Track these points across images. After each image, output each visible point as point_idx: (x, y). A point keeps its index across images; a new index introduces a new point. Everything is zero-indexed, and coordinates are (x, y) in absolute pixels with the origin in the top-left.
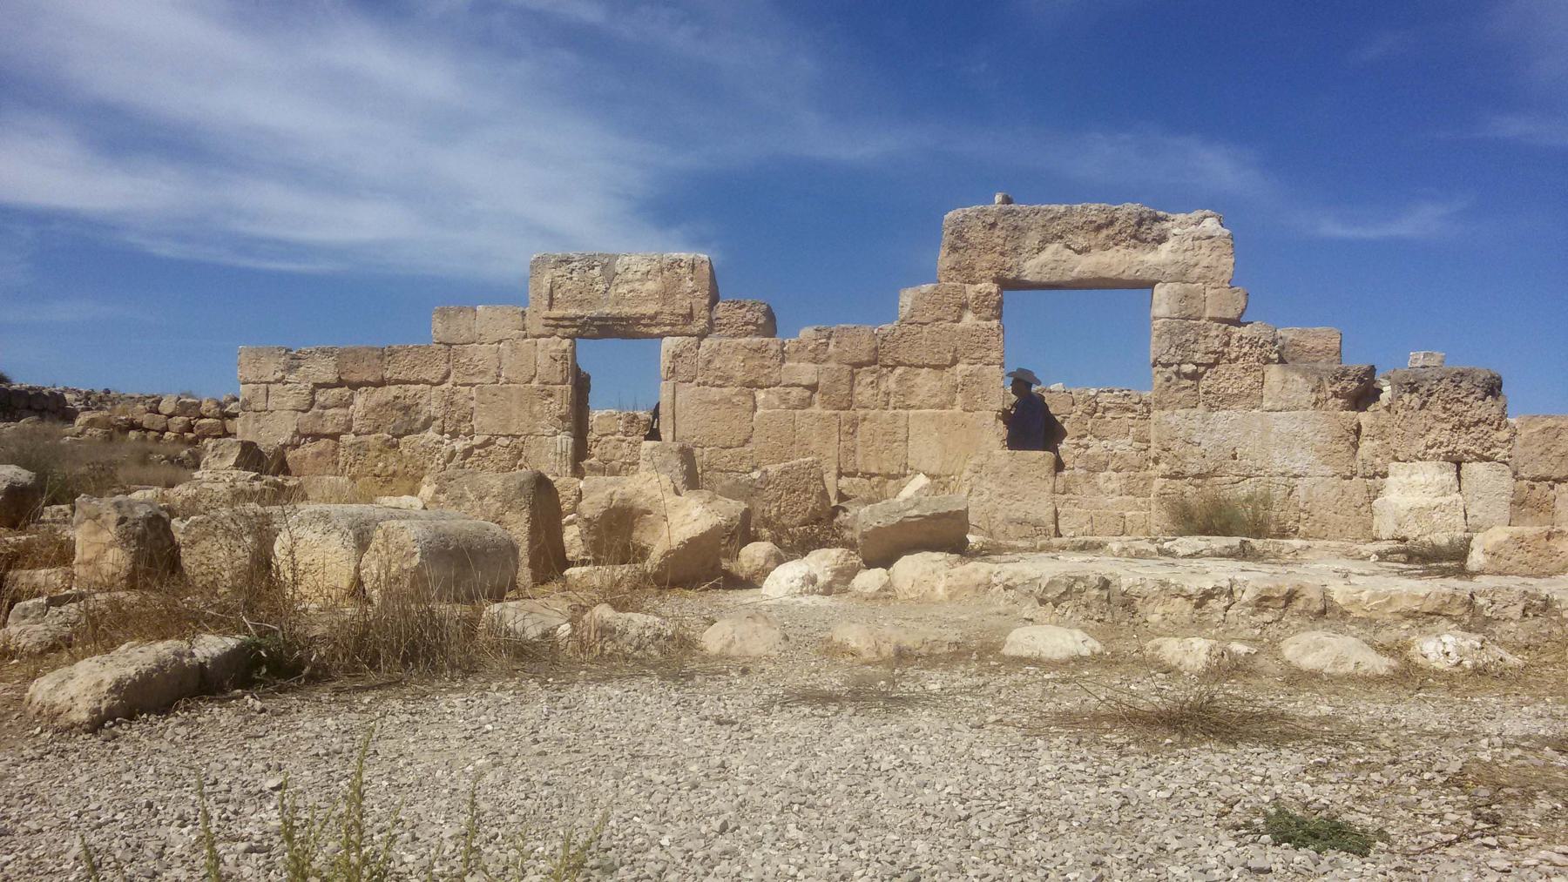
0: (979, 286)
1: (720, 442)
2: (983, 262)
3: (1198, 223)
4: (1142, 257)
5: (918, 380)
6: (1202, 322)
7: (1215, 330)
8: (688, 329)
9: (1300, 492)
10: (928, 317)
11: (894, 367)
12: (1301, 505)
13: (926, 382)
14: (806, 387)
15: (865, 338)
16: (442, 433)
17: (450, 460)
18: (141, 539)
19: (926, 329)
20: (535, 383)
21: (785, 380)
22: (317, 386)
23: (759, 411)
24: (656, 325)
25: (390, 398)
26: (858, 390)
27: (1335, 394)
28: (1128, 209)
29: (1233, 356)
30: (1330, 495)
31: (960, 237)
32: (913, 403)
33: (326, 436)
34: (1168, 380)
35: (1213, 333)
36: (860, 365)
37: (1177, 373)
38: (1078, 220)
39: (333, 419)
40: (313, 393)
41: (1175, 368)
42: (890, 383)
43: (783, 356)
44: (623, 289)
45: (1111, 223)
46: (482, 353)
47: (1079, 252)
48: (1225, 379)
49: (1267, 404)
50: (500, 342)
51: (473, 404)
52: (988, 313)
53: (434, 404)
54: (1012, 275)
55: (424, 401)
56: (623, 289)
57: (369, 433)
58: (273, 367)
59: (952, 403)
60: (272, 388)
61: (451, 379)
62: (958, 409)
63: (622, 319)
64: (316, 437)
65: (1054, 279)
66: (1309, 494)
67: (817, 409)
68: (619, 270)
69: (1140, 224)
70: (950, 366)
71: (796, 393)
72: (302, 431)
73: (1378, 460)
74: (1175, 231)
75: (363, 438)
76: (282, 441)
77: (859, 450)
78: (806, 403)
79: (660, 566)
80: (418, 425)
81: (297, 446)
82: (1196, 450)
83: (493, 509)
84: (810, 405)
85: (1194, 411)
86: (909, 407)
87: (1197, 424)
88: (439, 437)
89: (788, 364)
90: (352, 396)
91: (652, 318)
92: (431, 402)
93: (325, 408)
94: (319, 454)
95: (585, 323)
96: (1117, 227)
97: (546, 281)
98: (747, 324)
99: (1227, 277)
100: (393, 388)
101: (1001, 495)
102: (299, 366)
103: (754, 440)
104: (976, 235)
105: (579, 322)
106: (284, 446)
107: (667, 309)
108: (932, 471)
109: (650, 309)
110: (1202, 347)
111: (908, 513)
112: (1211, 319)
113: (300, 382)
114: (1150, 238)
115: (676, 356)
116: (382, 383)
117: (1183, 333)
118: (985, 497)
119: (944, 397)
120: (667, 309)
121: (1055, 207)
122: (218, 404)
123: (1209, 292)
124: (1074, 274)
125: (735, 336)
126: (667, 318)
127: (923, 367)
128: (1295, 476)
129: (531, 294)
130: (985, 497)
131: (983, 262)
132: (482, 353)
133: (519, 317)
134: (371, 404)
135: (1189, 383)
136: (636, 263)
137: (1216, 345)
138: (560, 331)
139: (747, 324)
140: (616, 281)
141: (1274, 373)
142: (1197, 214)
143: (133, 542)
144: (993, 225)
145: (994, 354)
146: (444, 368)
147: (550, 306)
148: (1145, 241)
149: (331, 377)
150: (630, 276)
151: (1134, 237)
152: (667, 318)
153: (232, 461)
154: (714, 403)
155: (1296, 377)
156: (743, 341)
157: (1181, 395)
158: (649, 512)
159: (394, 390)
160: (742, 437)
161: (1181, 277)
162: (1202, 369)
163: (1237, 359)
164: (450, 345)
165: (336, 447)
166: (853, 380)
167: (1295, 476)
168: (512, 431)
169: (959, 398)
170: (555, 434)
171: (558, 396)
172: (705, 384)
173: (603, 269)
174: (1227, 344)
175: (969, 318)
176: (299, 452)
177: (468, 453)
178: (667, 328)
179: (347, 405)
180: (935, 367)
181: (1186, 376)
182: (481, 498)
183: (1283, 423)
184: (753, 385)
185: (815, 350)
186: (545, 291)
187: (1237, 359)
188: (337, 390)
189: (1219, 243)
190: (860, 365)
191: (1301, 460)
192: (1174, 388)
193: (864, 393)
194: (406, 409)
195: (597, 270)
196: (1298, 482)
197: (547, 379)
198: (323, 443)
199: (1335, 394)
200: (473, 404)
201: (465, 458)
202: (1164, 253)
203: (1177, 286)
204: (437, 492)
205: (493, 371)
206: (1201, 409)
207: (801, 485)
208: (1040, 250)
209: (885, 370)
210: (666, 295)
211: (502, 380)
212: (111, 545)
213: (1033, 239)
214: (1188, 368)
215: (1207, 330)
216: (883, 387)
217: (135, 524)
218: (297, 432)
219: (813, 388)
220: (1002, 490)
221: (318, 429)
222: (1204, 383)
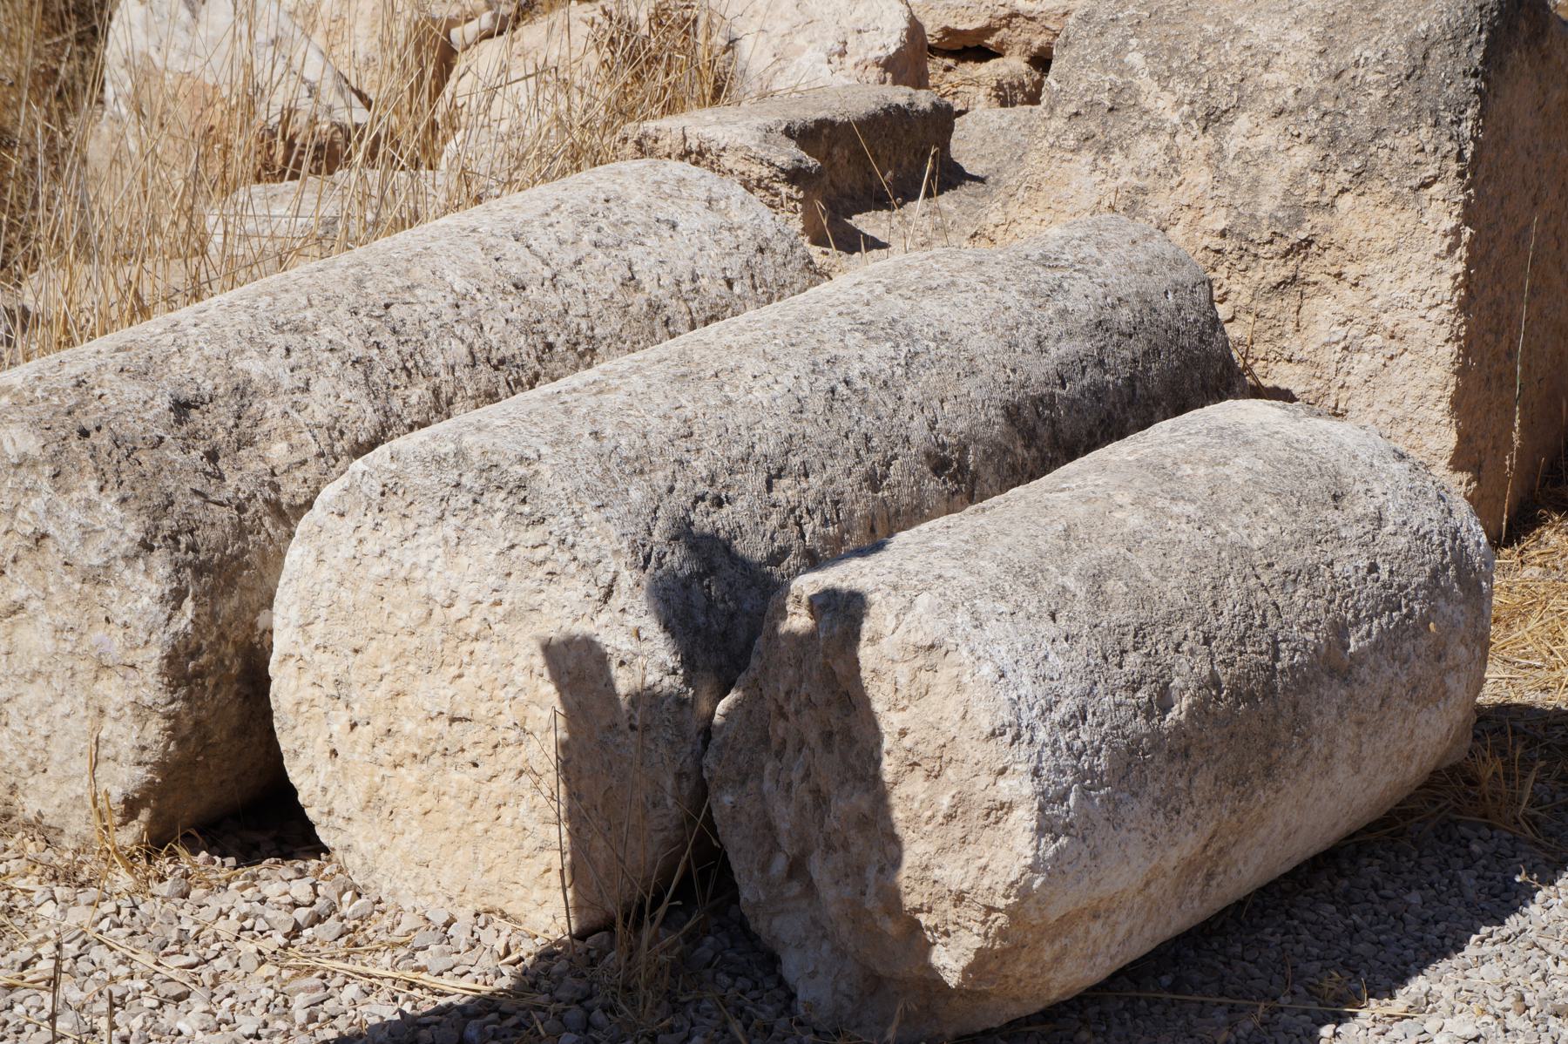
83: (1275, 181)
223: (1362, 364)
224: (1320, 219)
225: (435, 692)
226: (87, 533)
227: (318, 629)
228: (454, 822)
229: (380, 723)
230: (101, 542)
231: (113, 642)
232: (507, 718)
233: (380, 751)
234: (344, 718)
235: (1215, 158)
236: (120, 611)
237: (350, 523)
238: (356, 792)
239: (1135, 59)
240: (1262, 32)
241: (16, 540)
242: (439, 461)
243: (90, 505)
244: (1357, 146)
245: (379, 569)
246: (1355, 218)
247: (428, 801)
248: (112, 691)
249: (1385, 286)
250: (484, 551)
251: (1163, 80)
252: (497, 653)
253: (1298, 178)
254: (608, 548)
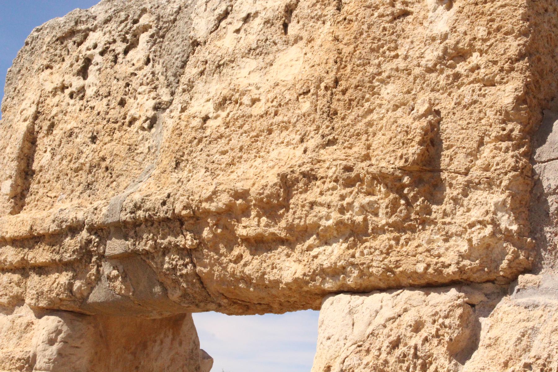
24: (295, 237)
63: (175, 223)
91: (272, 207)
105: (71, 244)
120: (332, 160)
126: (322, 204)
140: (191, 71)
147: (19, 199)
150: (228, 42)
173: (158, 37)
178: (334, 253)
210: (338, 95)
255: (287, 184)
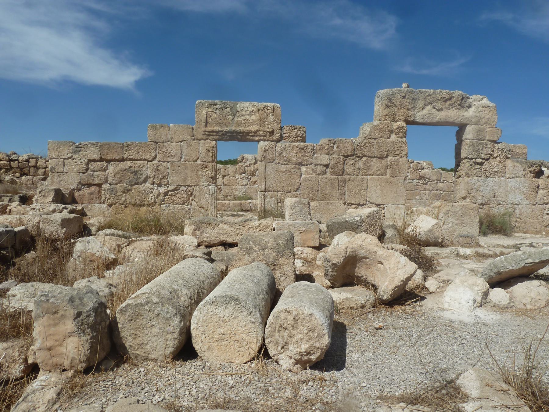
0: (398, 123)
1: (286, 190)
2: (400, 113)
3: (481, 100)
4: (462, 114)
5: (372, 163)
6: (485, 141)
7: (490, 145)
8: (272, 138)
9: (518, 211)
10: (377, 135)
11: (362, 157)
12: (518, 216)
13: (375, 164)
14: (324, 166)
15: (350, 144)
16: (153, 184)
17: (157, 197)
18: (93, 327)
19: (376, 141)
20: (199, 162)
21: (315, 162)
22: (90, 161)
23: (303, 176)
25: (127, 167)
26: (346, 167)
27: (531, 172)
28: (457, 93)
29: (495, 156)
30: (528, 212)
31: (390, 101)
32: (370, 173)
33: (95, 185)
34: (471, 165)
35: (489, 146)
36: (347, 156)
37: (475, 163)
38: (438, 97)
39: (98, 176)
40: (88, 164)
41: (474, 160)
42: (360, 164)
43: (314, 151)
44: (241, 119)
45: (451, 99)
46: (173, 147)
47: (438, 110)
48: (493, 165)
49: (507, 176)
50: (181, 142)
51: (168, 171)
52: (401, 135)
53: (149, 170)
54: (412, 119)
55: (144, 169)
56: (241, 119)
57: (117, 184)
58: (66, 151)
59: (386, 173)
60: (66, 161)
61: (157, 159)
62: (388, 176)
63: (241, 133)
64: (90, 185)
65: (429, 121)
66: (521, 211)
67: (328, 175)
68: (239, 110)
69: (462, 100)
70: (385, 158)
71: (319, 168)
72: (82, 182)
73: (545, 198)
74: (475, 103)
75: (114, 186)
76: (72, 187)
77: (346, 193)
78: (324, 173)
79: (391, 295)
80: (141, 180)
81: (80, 190)
82: (481, 194)
83: (272, 257)
84: (325, 173)
85: (480, 178)
86: (368, 175)
87: (482, 183)
88: (152, 186)
89: (316, 155)
90: (107, 166)
91: (255, 133)
92: (148, 170)
93: (94, 171)
94: (91, 194)
95: (223, 134)
96: (453, 100)
97: (204, 113)
98: (298, 136)
99: (494, 123)
100: (128, 162)
101: (457, 225)
102: (80, 151)
103: (301, 188)
104: (397, 101)
106: (73, 190)
107: (261, 129)
108: (377, 203)
109: (254, 128)
110: (485, 152)
111: (527, 261)
112: (489, 141)
113: (81, 159)
114: (465, 105)
115: (266, 150)
116: (122, 160)
117: (478, 146)
118: (450, 225)
119: (383, 171)
121: (427, 90)
122: (8, 155)
123: (488, 129)
124: (437, 119)
125: (292, 142)
126: (262, 133)
127: (374, 157)
128: (516, 204)
129: (196, 119)
130: (450, 225)
131: (400, 113)
132: (173, 147)
133: (191, 130)
134: (118, 169)
135: (479, 166)
136: (247, 107)
137: (489, 151)
138: (211, 138)
139: (298, 136)
140: (238, 114)
141: (509, 163)
142: (484, 96)
143: (89, 331)
144: (404, 97)
145: (404, 153)
146: (154, 153)
147: (206, 125)
148: (463, 107)
149: (97, 156)
150: (244, 113)
151: (460, 105)
152: (262, 133)
153: (51, 199)
154: (283, 172)
155: (518, 165)
156: (296, 144)
157: (475, 171)
158: (367, 258)
159: (129, 164)
160: (295, 188)
161: (478, 123)
162: (484, 161)
163: (497, 157)
164: (157, 143)
165: (100, 189)
166: (344, 163)
167: (516, 204)
168: (188, 183)
169: (389, 171)
170: (209, 185)
171: (210, 168)
172: (279, 163)
173: (231, 109)
174: (493, 151)
175: (393, 137)
176: (81, 192)
177: (166, 194)
178: (262, 138)
179: (105, 170)
180: (379, 158)
181: (478, 164)
182: (263, 250)
183: (512, 183)
184: (300, 164)
185: (328, 149)
186: (204, 118)
187: (497, 157)
188: (99, 163)
189: (492, 109)
190: (347, 156)
191: (519, 198)
192: (473, 168)
193: (349, 168)
194: (135, 173)
195: (228, 109)
196: (516, 206)
197: (205, 160)
198: (93, 189)
199: (531, 172)
200: (168, 171)
201: (165, 196)
202: (471, 112)
203: (476, 126)
204: (195, 230)
205: (178, 156)
206: (483, 177)
207: (374, 222)
208: (423, 109)
209: (358, 159)
210: (261, 122)
211: (183, 160)
212: (71, 334)
213: (420, 104)
214: (479, 160)
215: (487, 145)
216: (357, 166)
217: (88, 316)
218: (80, 183)
219: (327, 166)
220: (457, 222)
221: (91, 181)
222: (484, 167)
223: (283, 278)
224: (277, 261)
225: (222, 330)
226: (167, 313)
227: (200, 324)
228: (223, 349)
229: (211, 336)
230: (170, 314)
231: (171, 329)
232: (233, 333)
233: (210, 341)
234: (204, 336)
235: (264, 255)
236: (172, 324)
237: (206, 307)
238: (206, 347)
239: (251, 243)
240: (267, 239)
241: (154, 315)
242: (223, 297)
243: (168, 308)
244: (282, 252)
245: (212, 313)
246: (281, 261)
247: (219, 347)
248: (170, 336)
249: (286, 269)
250: (230, 309)
251: (255, 246)
252: (231, 324)
253: (274, 256)
254: (251, 306)
255: (257, 131)
